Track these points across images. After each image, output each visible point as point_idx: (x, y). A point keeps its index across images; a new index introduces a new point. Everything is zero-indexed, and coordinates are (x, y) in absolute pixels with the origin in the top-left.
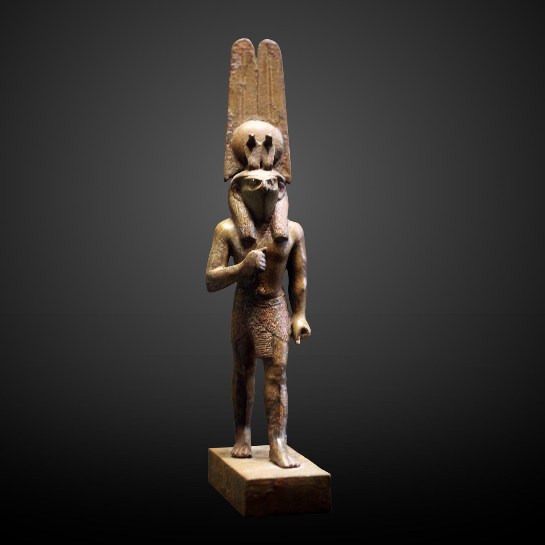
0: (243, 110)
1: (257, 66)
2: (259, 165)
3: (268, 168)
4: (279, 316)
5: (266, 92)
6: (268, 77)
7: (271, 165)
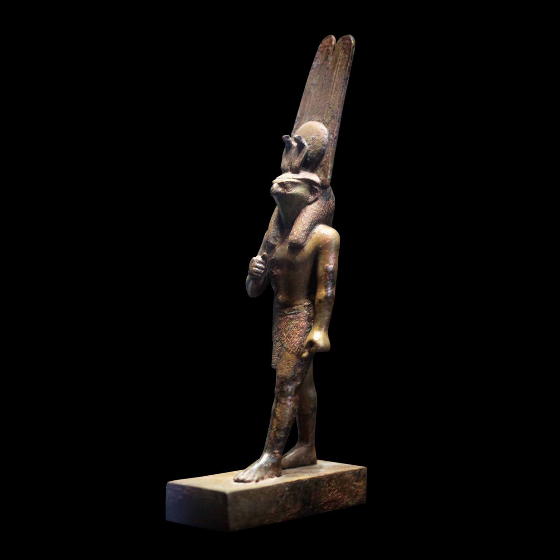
0: (307, 111)
1: (330, 64)
2: (289, 167)
3: (296, 171)
4: (292, 326)
5: (329, 91)
6: (335, 74)
7: (296, 167)
